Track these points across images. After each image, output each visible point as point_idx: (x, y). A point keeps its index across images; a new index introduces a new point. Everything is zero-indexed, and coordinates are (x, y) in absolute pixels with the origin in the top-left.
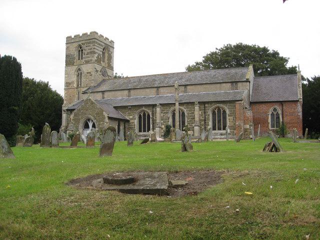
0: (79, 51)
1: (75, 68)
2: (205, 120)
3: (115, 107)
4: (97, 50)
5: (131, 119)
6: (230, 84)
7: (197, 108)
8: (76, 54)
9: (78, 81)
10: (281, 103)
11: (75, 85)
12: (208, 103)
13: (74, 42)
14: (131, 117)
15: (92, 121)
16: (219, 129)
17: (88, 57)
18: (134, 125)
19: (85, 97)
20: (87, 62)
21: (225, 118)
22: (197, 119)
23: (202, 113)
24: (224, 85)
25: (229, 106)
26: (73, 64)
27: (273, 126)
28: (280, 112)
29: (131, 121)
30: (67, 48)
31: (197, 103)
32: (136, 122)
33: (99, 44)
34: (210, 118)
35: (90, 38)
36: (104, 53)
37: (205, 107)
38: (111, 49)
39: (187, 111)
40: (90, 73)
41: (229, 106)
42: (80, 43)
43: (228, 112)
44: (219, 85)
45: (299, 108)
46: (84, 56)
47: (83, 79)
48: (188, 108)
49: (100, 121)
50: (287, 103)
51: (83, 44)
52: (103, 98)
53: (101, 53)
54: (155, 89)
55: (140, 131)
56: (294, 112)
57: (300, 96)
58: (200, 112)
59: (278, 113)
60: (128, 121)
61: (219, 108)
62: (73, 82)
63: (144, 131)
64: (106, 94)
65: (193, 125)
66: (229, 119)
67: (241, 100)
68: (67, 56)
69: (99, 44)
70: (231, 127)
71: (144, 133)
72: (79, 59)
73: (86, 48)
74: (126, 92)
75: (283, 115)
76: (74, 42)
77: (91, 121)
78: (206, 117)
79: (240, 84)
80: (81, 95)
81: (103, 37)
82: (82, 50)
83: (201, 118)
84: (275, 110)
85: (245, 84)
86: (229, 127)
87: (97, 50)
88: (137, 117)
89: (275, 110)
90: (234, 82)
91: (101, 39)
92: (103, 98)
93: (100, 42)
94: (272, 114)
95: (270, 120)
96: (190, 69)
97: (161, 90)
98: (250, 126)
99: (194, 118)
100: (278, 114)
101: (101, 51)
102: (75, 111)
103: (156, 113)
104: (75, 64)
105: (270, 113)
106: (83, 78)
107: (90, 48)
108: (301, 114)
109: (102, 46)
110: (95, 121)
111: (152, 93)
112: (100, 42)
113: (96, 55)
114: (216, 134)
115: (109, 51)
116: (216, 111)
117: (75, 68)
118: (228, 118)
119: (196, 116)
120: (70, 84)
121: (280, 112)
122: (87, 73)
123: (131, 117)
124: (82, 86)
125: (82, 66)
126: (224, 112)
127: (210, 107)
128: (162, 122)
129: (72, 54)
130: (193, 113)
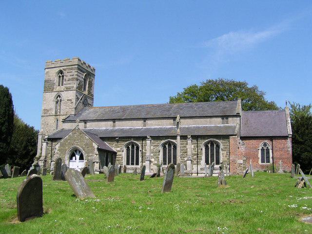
0: (60, 77)
1: (54, 94)
2: (198, 154)
3: (100, 138)
5: (119, 151)
7: (189, 141)
8: (56, 80)
10: (271, 138)
11: (54, 113)
14: (119, 149)
15: (80, 152)
17: (69, 84)
19: (68, 126)
20: (68, 89)
21: (218, 153)
22: (189, 153)
23: (194, 147)
27: (263, 161)
28: (270, 148)
31: (190, 136)
32: (124, 154)
35: (69, 64)
36: (85, 80)
40: (71, 100)
42: (61, 68)
43: (221, 147)
45: (289, 143)
46: (64, 82)
47: (63, 107)
49: (89, 153)
51: (64, 70)
52: (85, 127)
53: (83, 80)
57: (290, 131)
58: (193, 146)
59: (267, 148)
60: (115, 153)
61: (212, 142)
62: (51, 109)
63: (133, 164)
64: (88, 124)
65: (186, 159)
66: (223, 154)
67: (235, 135)
71: (133, 166)
74: (111, 123)
75: (272, 149)
77: (78, 152)
78: (199, 151)
79: (230, 119)
80: (60, 123)
82: (63, 76)
85: (235, 118)
88: (125, 150)
89: (265, 145)
90: (225, 116)
92: (85, 127)
94: (263, 150)
95: (260, 155)
96: (172, 101)
97: (148, 122)
98: (244, 161)
100: (268, 150)
102: (62, 141)
103: (145, 146)
104: (54, 90)
105: (260, 148)
108: (290, 149)
109: (84, 72)
110: (83, 152)
111: (138, 125)
116: (209, 145)
118: (221, 152)
119: (188, 150)
120: (48, 111)
121: (270, 148)
122: (68, 100)
123: (119, 149)
124: (62, 113)
125: (62, 93)
128: (152, 155)
129: (52, 79)
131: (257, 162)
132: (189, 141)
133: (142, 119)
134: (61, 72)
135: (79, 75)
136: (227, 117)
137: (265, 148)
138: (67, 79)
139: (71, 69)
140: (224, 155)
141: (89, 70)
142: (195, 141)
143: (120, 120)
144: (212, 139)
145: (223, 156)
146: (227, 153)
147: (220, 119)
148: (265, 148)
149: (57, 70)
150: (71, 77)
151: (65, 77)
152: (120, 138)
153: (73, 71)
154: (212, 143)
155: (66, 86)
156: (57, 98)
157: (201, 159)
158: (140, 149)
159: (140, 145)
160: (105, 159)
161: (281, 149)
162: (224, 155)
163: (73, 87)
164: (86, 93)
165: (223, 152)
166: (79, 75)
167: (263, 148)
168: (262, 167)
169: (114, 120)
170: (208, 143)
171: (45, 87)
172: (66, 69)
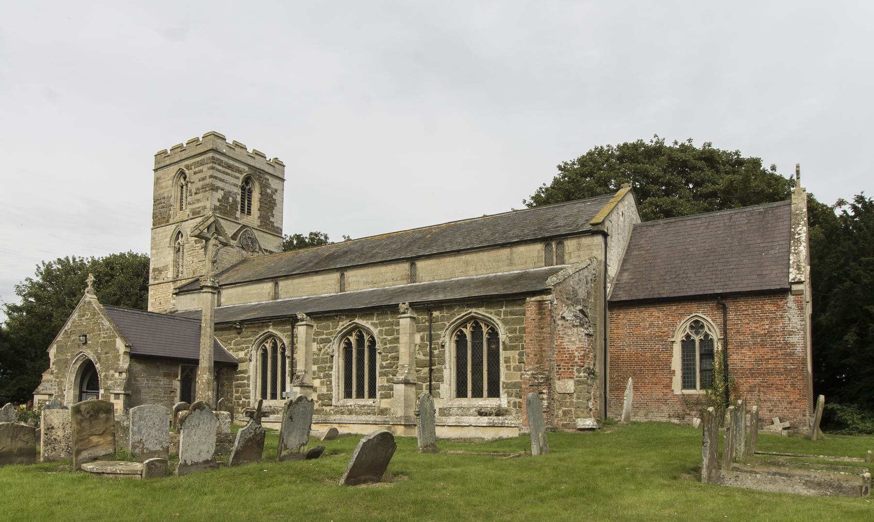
1: (170, 229)
2: (431, 364)
4: (222, 180)
6: (539, 247)
7: (405, 322)
9: (176, 264)
11: (170, 275)
12: (439, 305)
13: (170, 165)
14: (241, 354)
16: (478, 393)
17: (198, 201)
18: (248, 378)
21: (494, 357)
23: (422, 339)
24: (522, 249)
25: (506, 313)
26: (168, 221)
28: (715, 334)
29: (242, 366)
30: (157, 181)
33: (229, 167)
34: (447, 355)
35: (198, 152)
36: (246, 192)
37: (431, 321)
38: (274, 183)
39: (380, 332)
41: (506, 313)
43: (503, 335)
44: (505, 252)
48: (382, 324)
50: (742, 305)
51: (188, 167)
54: (336, 276)
55: (348, 395)
56: (770, 334)
58: (417, 338)
59: (706, 335)
61: (477, 323)
62: (166, 268)
66: (507, 360)
68: (156, 201)
69: (229, 167)
70: (516, 389)
72: (181, 209)
73: (196, 178)
74: (268, 287)
76: (170, 165)
78: (436, 352)
79: (570, 245)
81: (244, 148)
83: (421, 357)
84: (697, 326)
86: (507, 386)
87: (222, 180)
89: (697, 326)
90: (552, 238)
91: (237, 153)
93: (231, 162)
94: (687, 344)
95: (677, 363)
98: (578, 383)
99: (398, 359)
100: (707, 342)
101: (236, 185)
104: (171, 221)
105: (679, 337)
106: (186, 254)
107: (200, 175)
109: (240, 172)
112: (231, 162)
113: (220, 194)
114: (464, 410)
115: (264, 186)
117: (170, 229)
118: (503, 354)
121: (715, 334)
126: (494, 334)
127: (448, 319)
128: (315, 368)
129: (166, 195)
130: (397, 340)
131: (669, 386)
132: (405, 322)
133: (338, 270)
134: (182, 173)
135: (220, 175)
136: (560, 239)
137: (697, 339)
138: (194, 191)
139: (201, 163)
140: (512, 364)
141: (258, 163)
142: (423, 317)
143: (287, 277)
144: (474, 311)
145: (508, 368)
146: (521, 354)
147: (538, 249)
148: (697, 339)
149: (175, 168)
150: (201, 183)
151: (189, 185)
152: (242, 322)
153: (205, 168)
154: (476, 323)
155: (190, 207)
156: (177, 238)
157: (441, 379)
158: (287, 353)
159: (286, 341)
160: (177, 384)
161: (764, 340)
162: (512, 364)
163: (205, 208)
164: (253, 219)
165: (509, 353)
166: (220, 175)
167: (688, 336)
168: (685, 401)
169: (275, 279)
170: (464, 324)
171: (155, 216)
172: (191, 165)
